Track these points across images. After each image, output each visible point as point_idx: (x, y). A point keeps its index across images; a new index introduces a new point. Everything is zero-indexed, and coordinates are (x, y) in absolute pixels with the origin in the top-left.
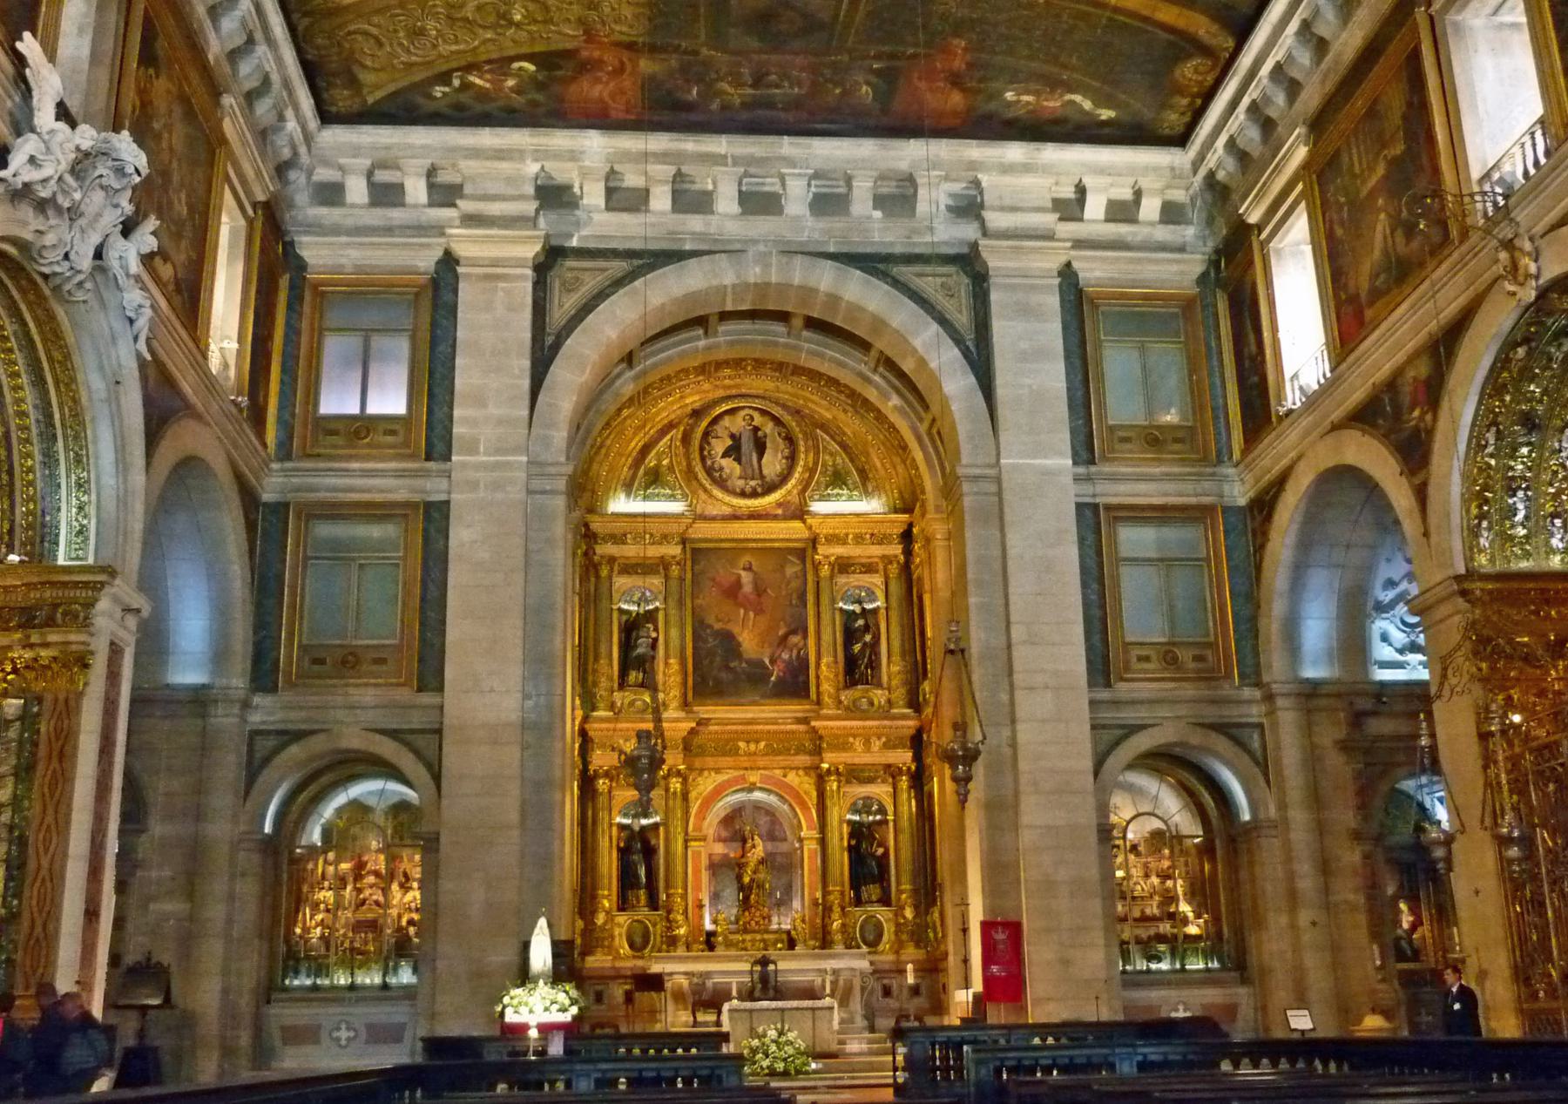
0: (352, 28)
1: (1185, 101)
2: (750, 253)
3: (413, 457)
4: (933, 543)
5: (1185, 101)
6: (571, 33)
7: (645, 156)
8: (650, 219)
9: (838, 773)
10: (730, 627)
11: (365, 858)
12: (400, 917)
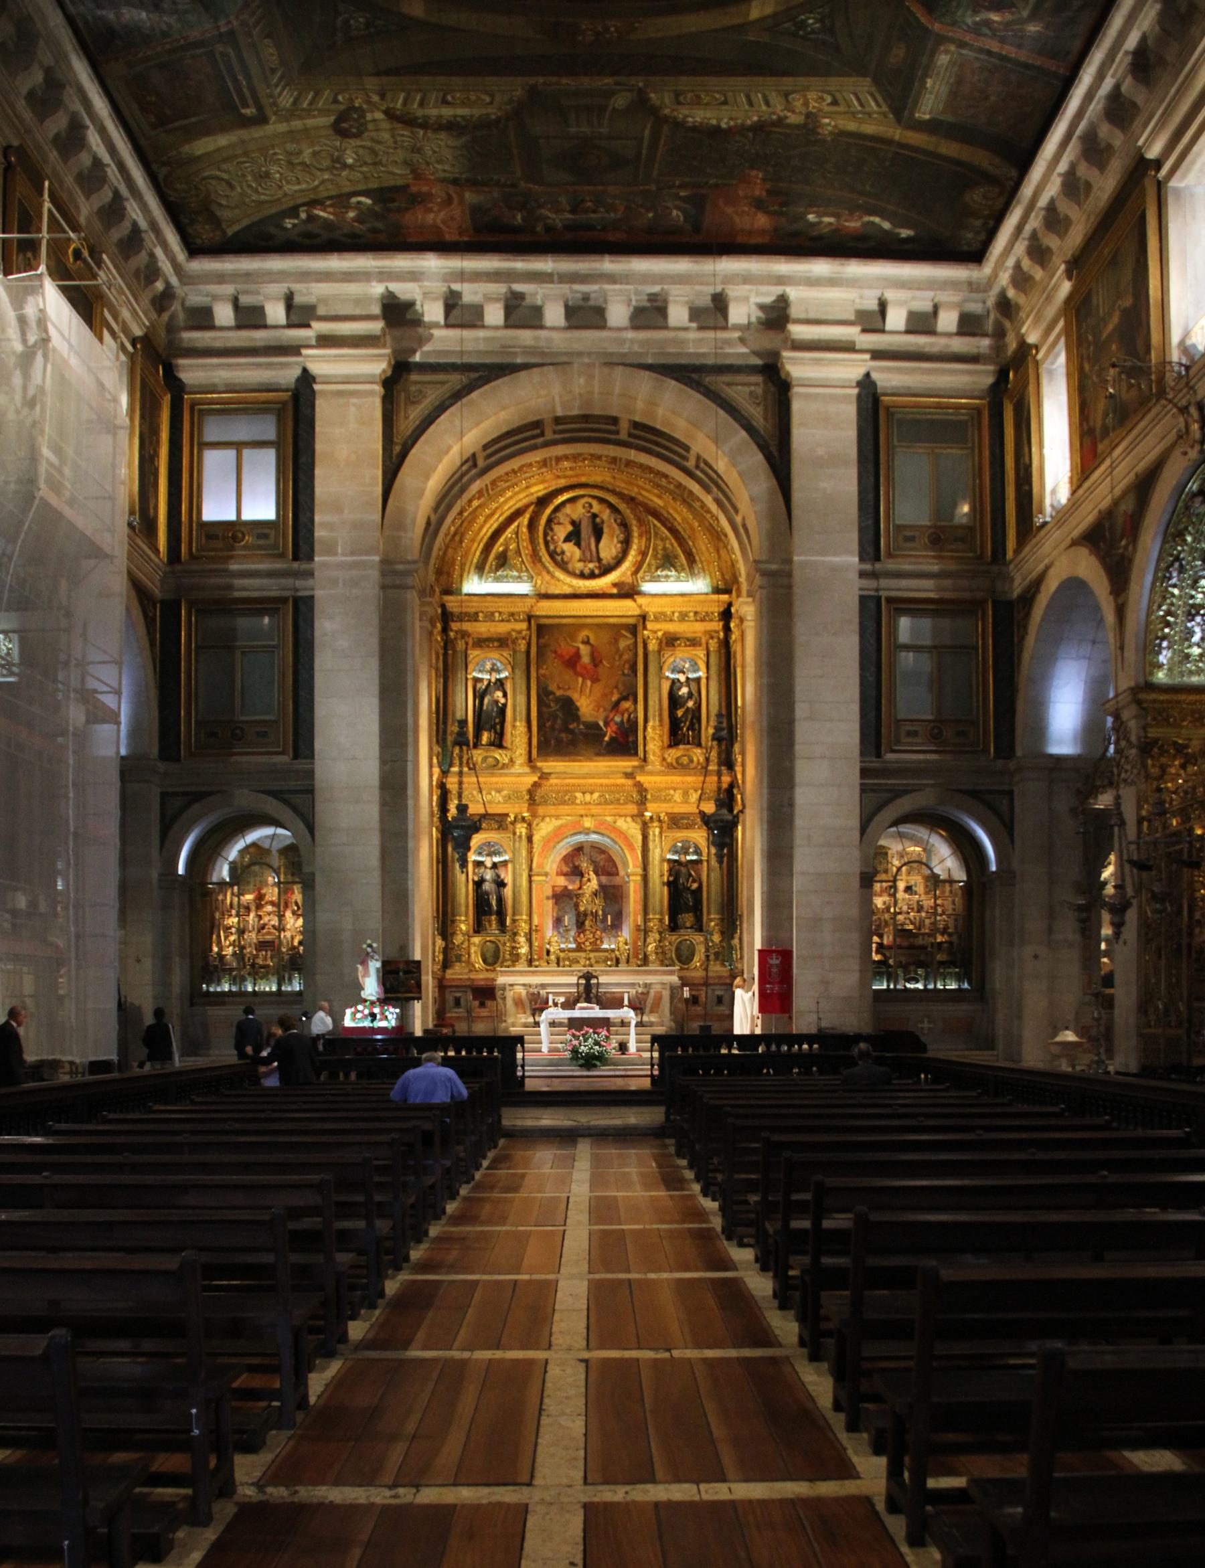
0: (206, 174)
3: (282, 556)
4: (746, 624)
6: (398, 172)
7: (476, 277)
9: (660, 821)
10: (569, 693)
11: (263, 891)
12: (293, 938)
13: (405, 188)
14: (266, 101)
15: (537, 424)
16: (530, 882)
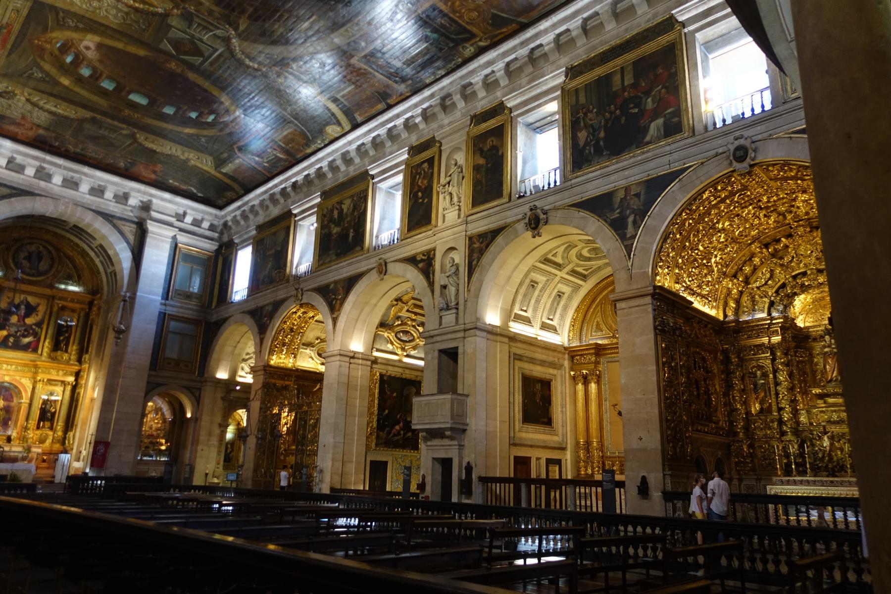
1: (225, 200)
2: (62, 201)
5: (225, 200)
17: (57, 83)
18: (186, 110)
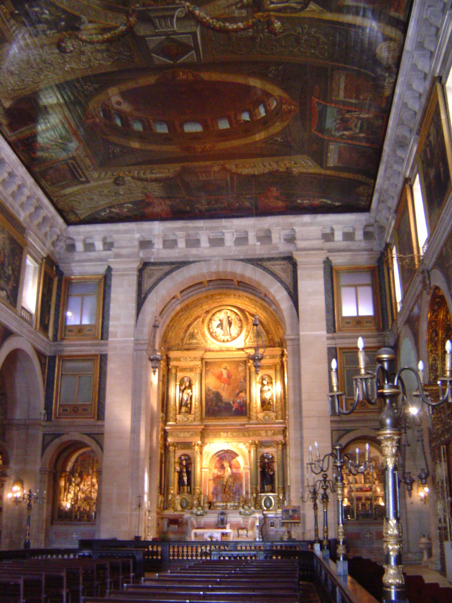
0: (70, 199)
1: (365, 198)
3: (97, 338)
5: (365, 198)
8: (176, 250)
13: (143, 201)
14: (88, 176)
15: (201, 283)
16: (201, 472)
17: (133, 151)
18: (235, 117)
